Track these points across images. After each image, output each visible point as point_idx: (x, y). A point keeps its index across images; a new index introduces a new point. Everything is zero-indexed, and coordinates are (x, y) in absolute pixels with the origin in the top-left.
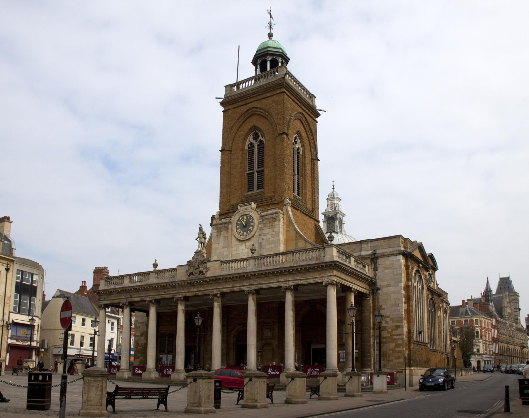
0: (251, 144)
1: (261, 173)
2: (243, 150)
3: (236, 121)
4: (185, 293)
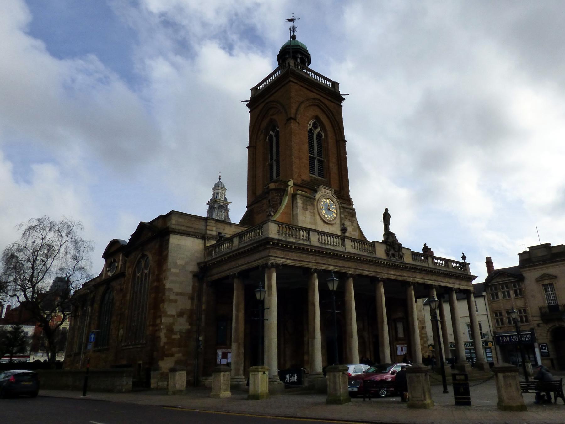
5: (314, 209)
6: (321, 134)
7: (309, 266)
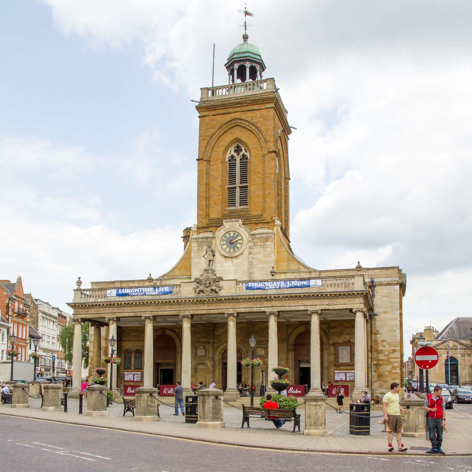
0: (232, 157)
1: (244, 189)
2: (223, 162)
3: (216, 130)
4: (193, 311)
6: (247, 156)
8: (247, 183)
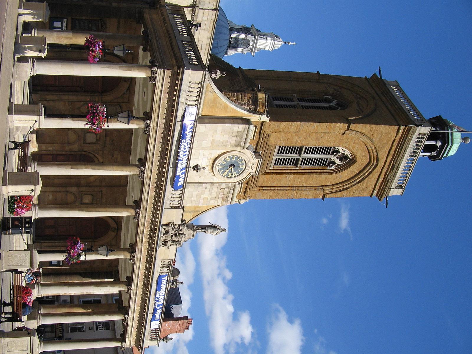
5: (231, 146)
6: (332, 166)
7: (154, 118)
8: (301, 164)
